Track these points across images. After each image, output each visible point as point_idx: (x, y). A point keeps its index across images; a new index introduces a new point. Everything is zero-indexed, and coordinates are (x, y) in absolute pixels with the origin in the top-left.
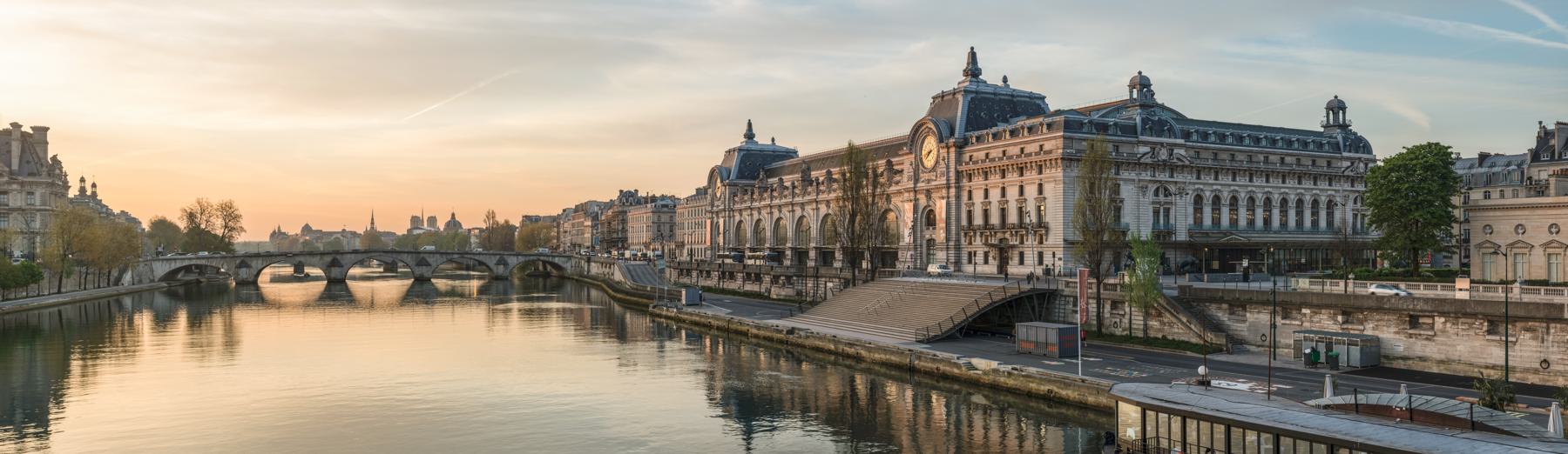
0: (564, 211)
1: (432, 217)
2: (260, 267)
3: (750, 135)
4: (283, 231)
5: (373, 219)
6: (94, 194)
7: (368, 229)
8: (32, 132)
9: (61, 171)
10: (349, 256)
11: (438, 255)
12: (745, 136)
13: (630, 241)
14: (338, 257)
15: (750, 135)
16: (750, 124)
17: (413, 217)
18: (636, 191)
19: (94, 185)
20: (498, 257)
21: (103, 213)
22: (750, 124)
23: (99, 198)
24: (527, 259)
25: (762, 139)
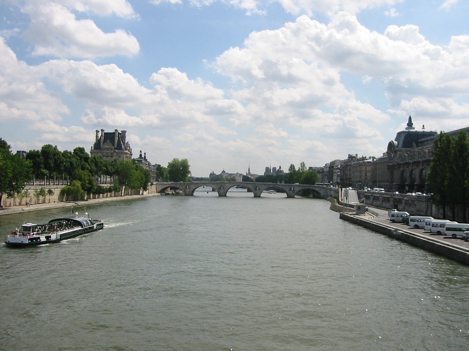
0: (326, 165)
1: (274, 168)
2: (194, 188)
3: (410, 124)
4: (214, 173)
5: (249, 168)
6: (145, 157)
7: (247, 173)
8: (121, 133)
9: (130, 148)
10: (227, 184)
11: (264, 186)
12: (408, 124)
13: (352, 180)
14: (223, 184)
15: (410, 124)
16: (410, 118)
17: (266, 168)
18: (357, 155)
19: (145, 154)
20: (290, 187)
21: (147, 165)
22: (410, 118)
23: (146, 158)
24: (303, 188)
25: (417, 127)
